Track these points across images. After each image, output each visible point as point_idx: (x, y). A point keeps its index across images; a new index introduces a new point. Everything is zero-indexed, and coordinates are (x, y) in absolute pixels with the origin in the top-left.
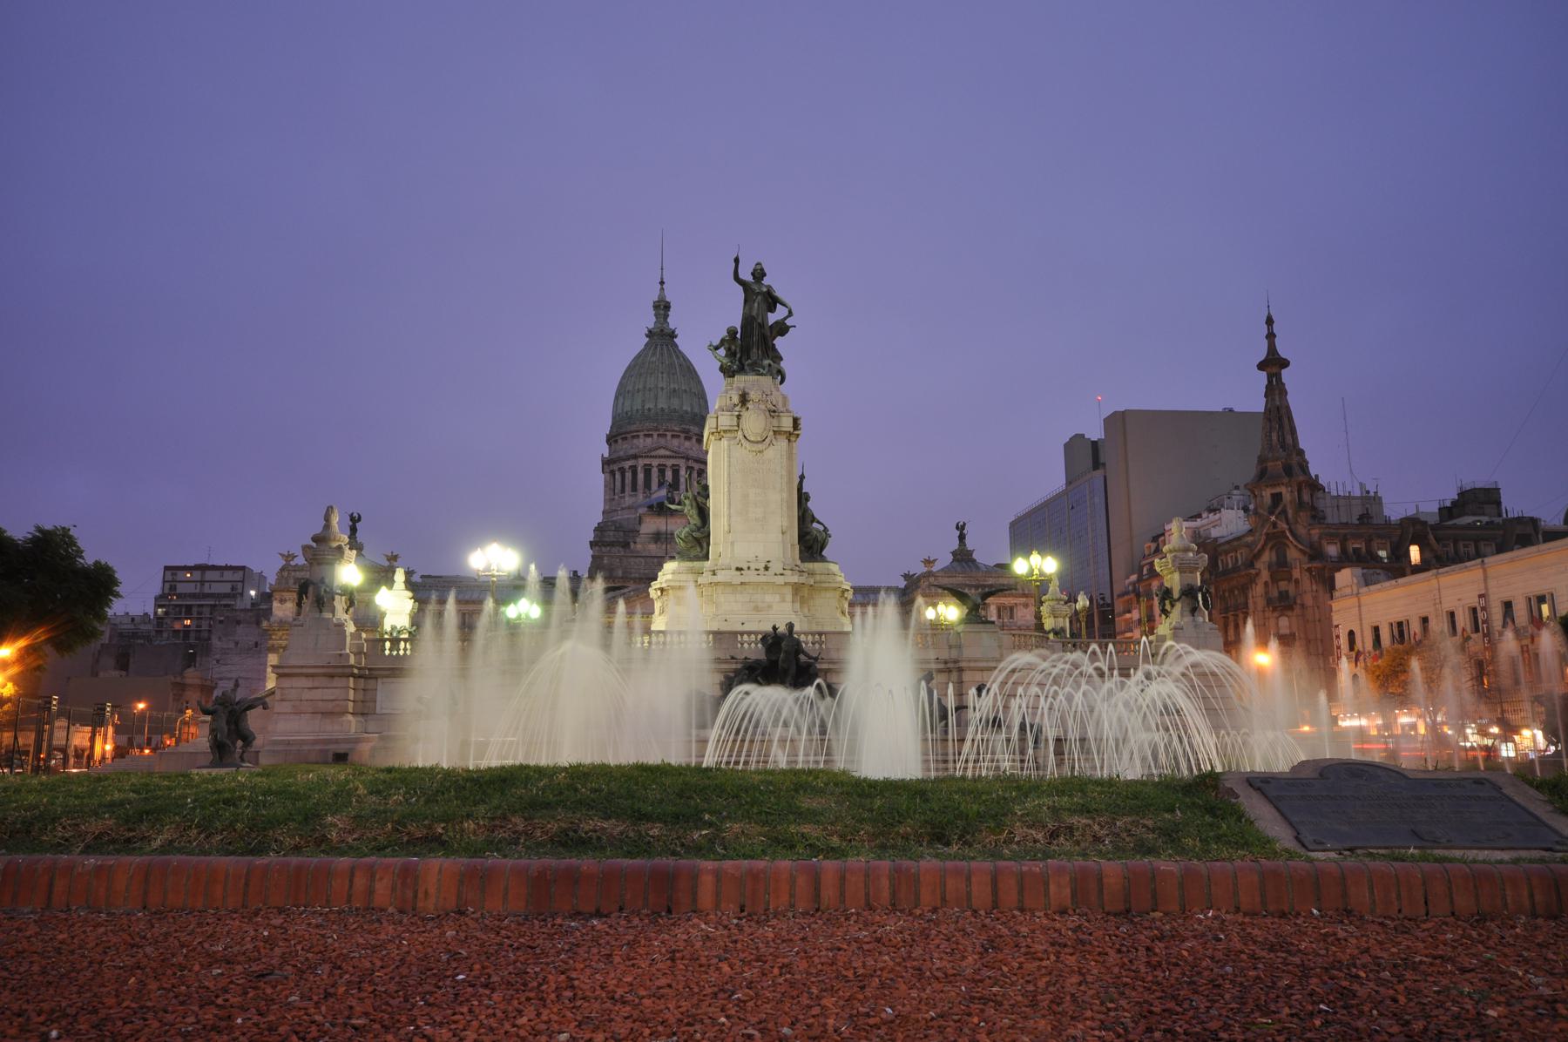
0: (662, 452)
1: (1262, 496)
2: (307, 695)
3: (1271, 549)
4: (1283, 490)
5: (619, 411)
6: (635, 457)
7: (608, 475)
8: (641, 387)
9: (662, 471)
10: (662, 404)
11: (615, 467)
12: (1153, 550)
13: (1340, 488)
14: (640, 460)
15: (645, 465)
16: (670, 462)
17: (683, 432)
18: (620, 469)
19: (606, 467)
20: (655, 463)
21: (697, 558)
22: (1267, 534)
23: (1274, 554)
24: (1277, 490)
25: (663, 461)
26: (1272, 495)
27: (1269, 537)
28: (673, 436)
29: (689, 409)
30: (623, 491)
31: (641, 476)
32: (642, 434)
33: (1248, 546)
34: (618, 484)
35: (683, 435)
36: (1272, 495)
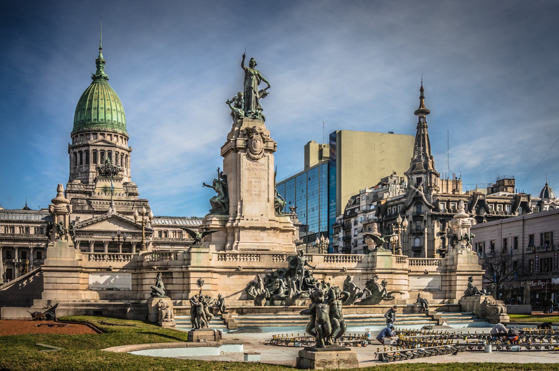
1: (412, 179)
2: (59, 280)
3: (415, 205)
4: (422, 176)
5: (78, 120)
7: (72, 155)
9: (103, 153)
11: (77, 150)
12: (352, 203)
13: (444, 176)
14: (90, 147)
15: (94, 150)
17: (114, 133)
18: (79, 152)
19: (71, 150)
21: (224, 214)
22: (414, 198)
23: (415, 208)
24: (419, 176)
25: (103, 148)
26: (417, 178)
27: (414, 199)
28: (108, 134)
30: (81, 163)
31: (91, 156)
32: (92, 132)
33: (403, 203)
34: (79, 159)
35: (113, 134)
36: (417, 178)
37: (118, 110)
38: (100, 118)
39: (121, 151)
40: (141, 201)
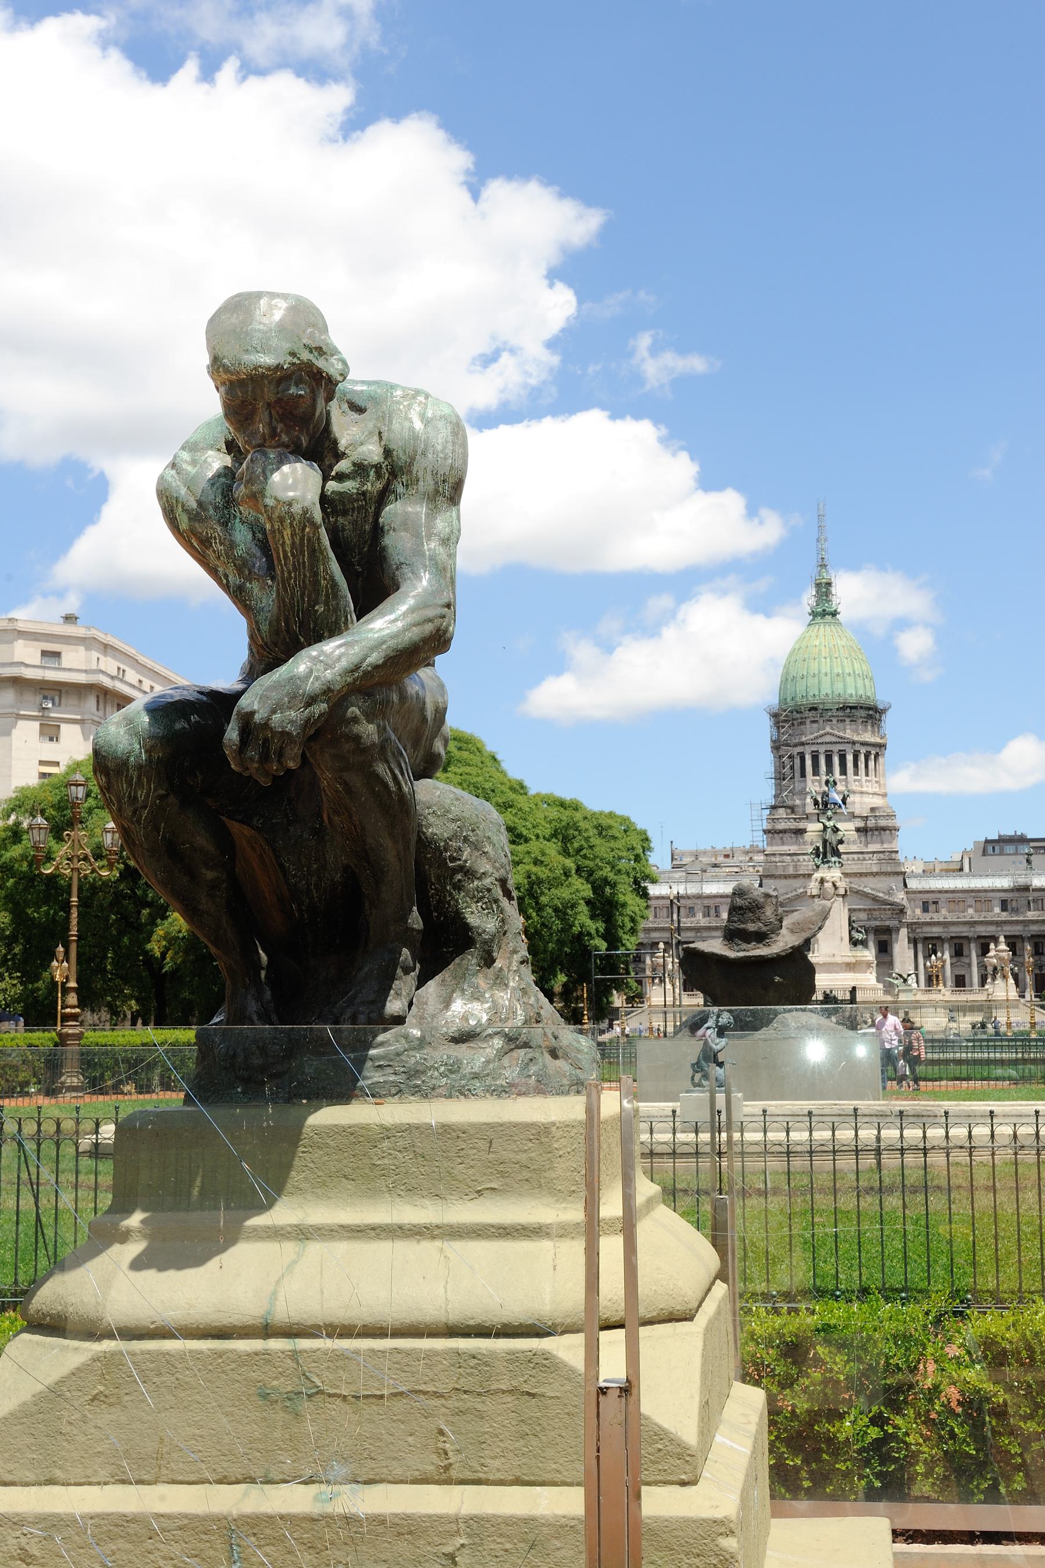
0: (828, 739)
6: (803, 744)
8: (805, 674)
10: (826, 689)
15: (812, 752)
16: (836, 748)
20: (822, 749)
25: (829, 747)
29: (854, 693)
37: (857, 672)
38: (823, 692)
39: (863, 750)
40: (884, 852)
